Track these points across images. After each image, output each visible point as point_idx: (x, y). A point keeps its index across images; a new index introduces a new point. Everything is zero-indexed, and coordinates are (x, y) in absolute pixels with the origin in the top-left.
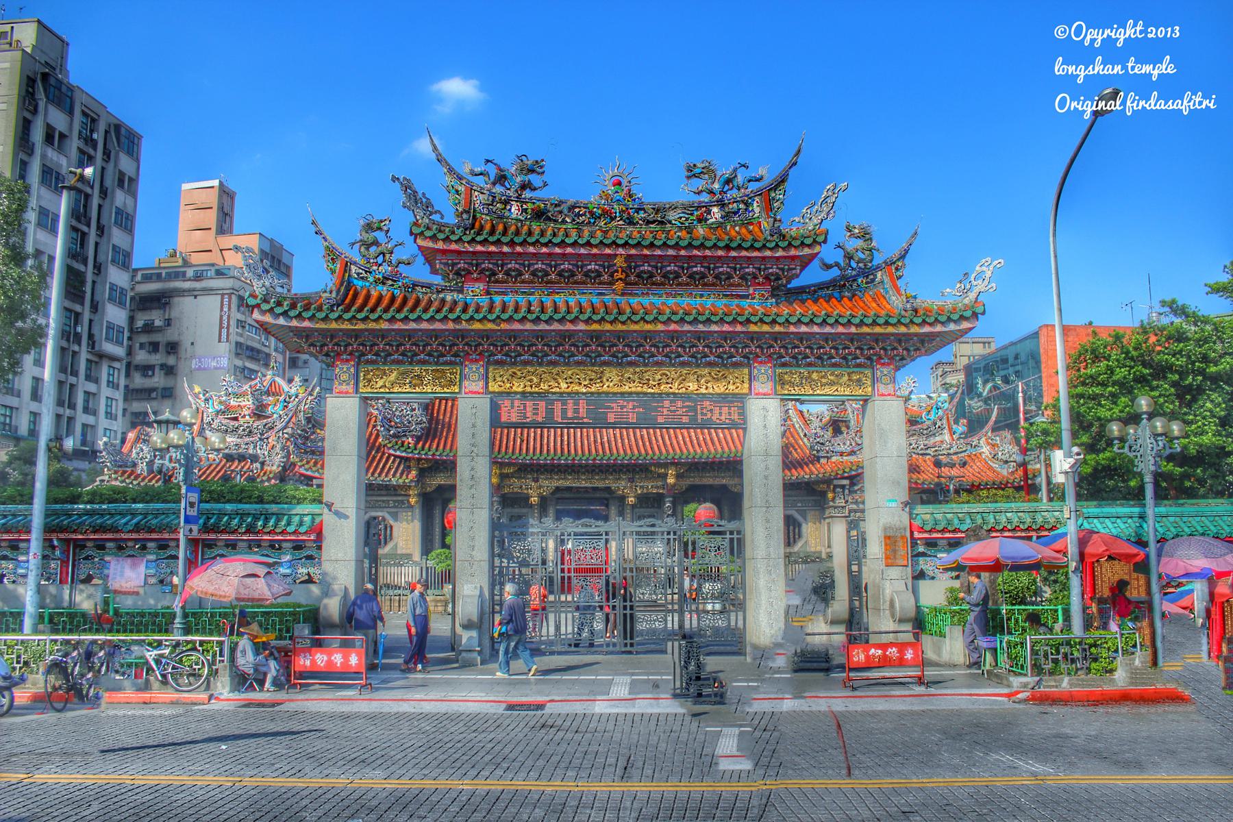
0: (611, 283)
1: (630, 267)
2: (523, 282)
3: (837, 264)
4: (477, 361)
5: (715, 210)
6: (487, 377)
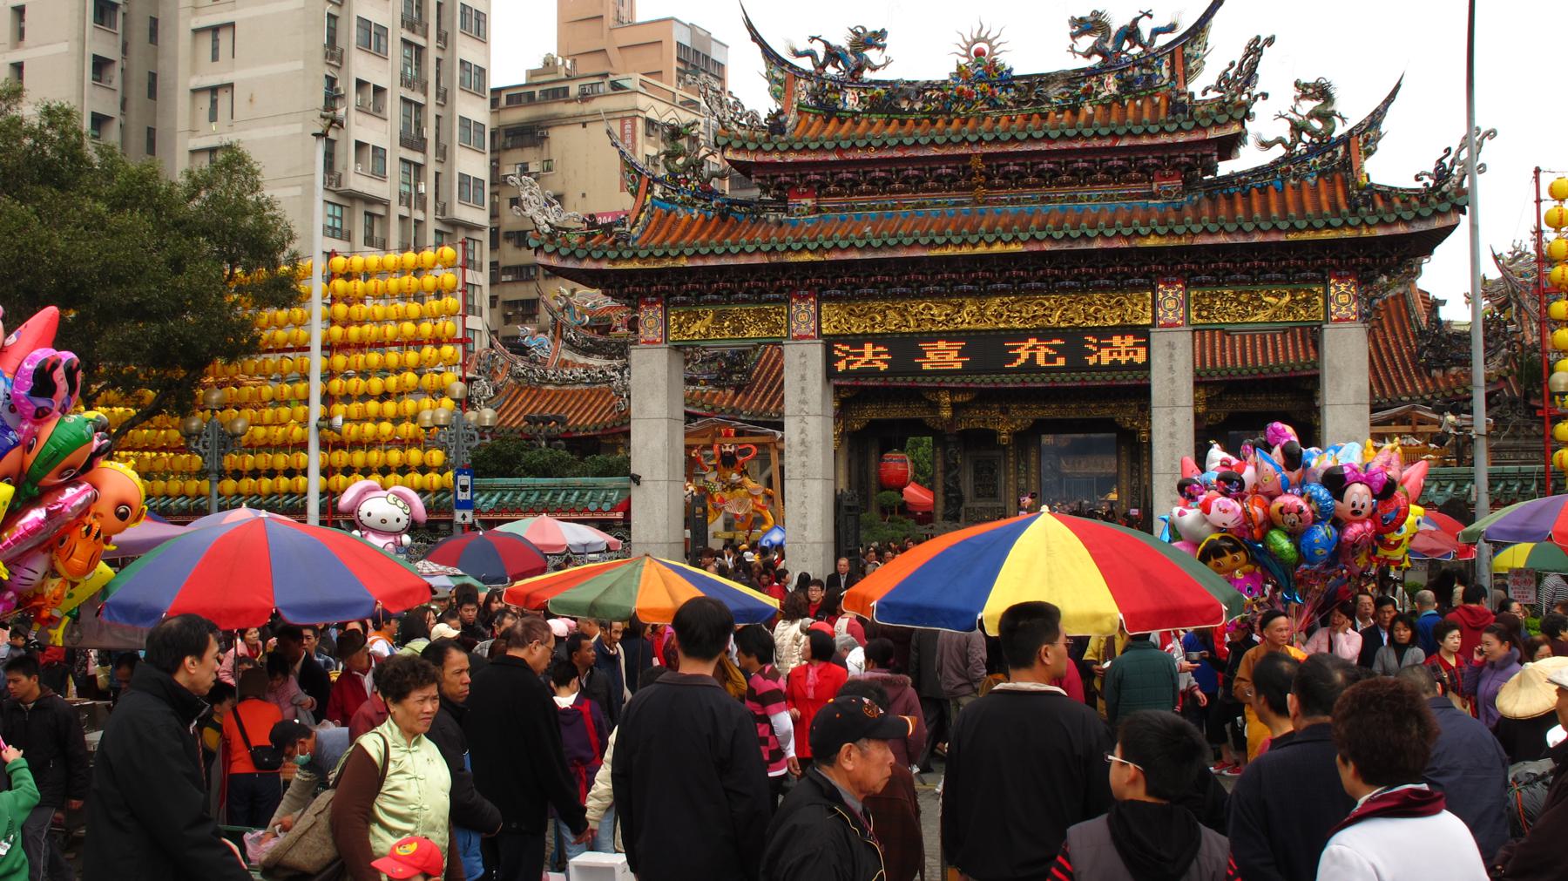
2: (861, 193)
3: (1281, 141)
4: (804, 298)
6: (819, 317)
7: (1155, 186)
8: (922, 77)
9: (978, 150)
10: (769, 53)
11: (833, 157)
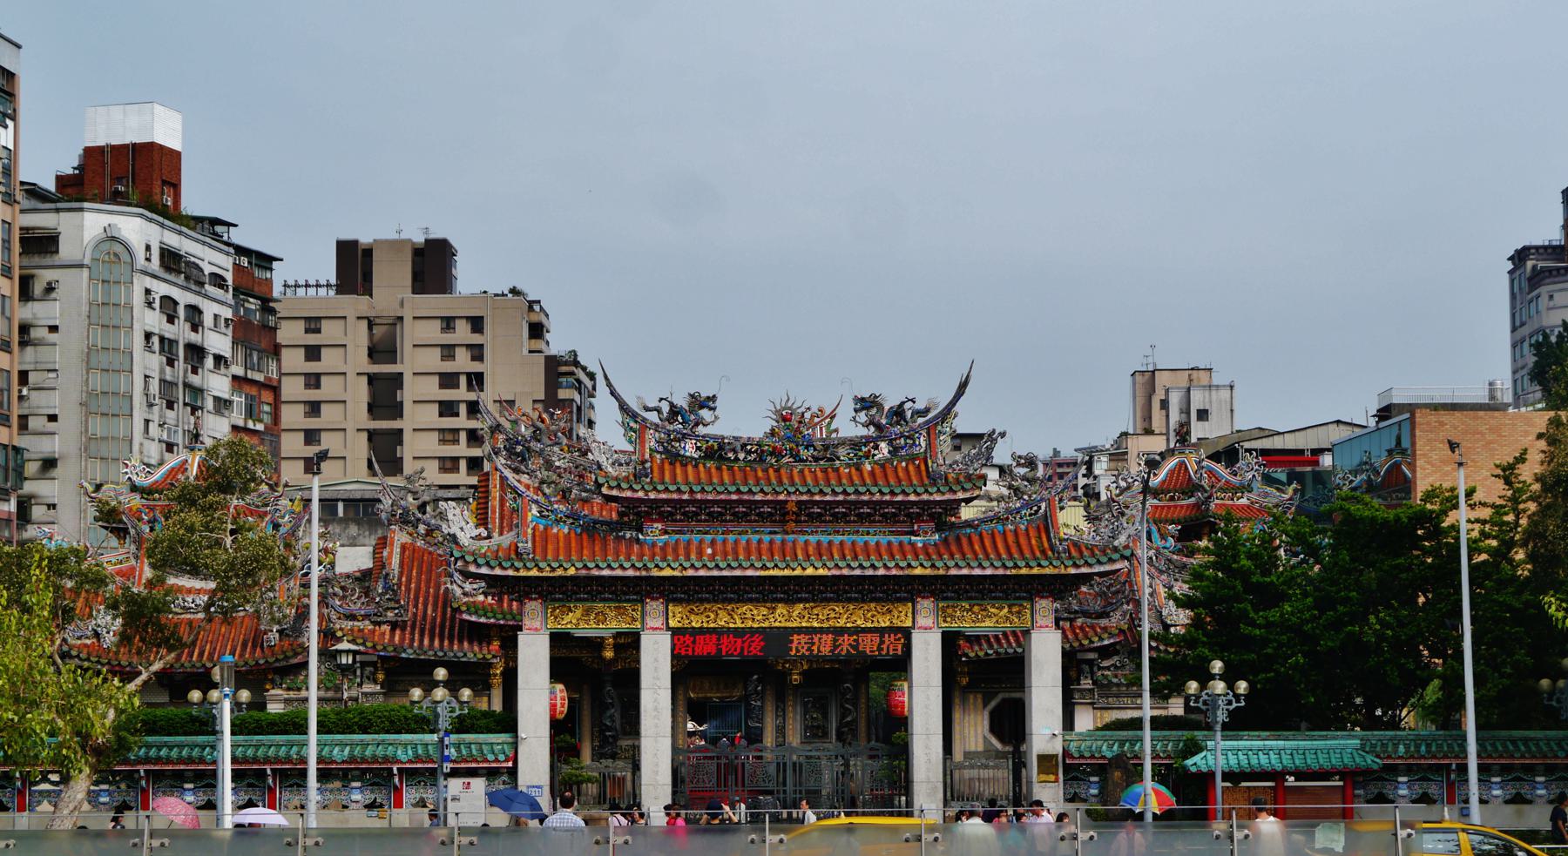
0: (783, 522)
5: (883, 445)
8: (744, 434)
9: (794, 498)
10: (624, 408)
11: (686, 497)
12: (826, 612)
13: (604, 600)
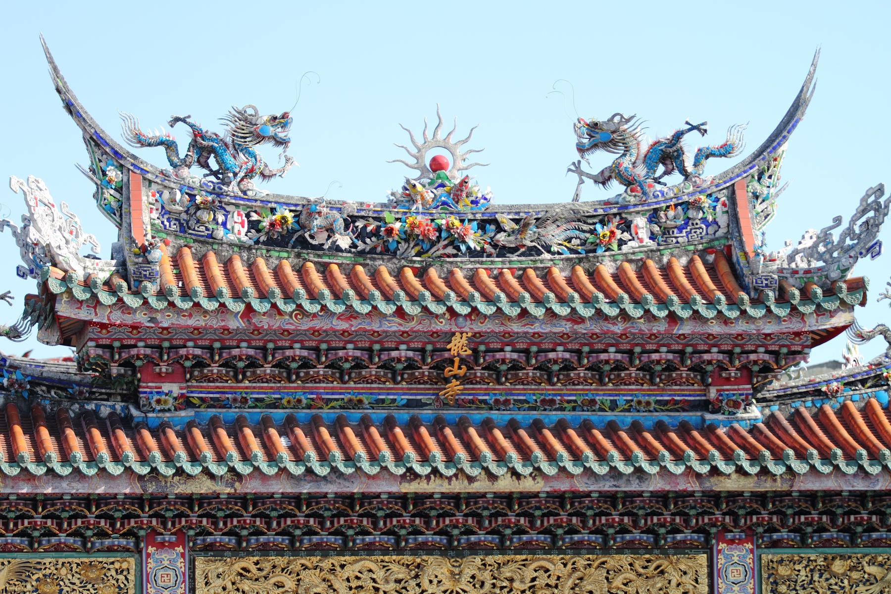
1: (475, 351)
5: (640, 222)
6: (193, 579)
7: (713, 393)
12: (529, 573)
13: (58, 549)
